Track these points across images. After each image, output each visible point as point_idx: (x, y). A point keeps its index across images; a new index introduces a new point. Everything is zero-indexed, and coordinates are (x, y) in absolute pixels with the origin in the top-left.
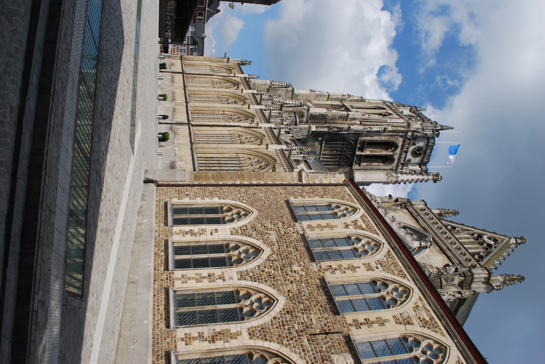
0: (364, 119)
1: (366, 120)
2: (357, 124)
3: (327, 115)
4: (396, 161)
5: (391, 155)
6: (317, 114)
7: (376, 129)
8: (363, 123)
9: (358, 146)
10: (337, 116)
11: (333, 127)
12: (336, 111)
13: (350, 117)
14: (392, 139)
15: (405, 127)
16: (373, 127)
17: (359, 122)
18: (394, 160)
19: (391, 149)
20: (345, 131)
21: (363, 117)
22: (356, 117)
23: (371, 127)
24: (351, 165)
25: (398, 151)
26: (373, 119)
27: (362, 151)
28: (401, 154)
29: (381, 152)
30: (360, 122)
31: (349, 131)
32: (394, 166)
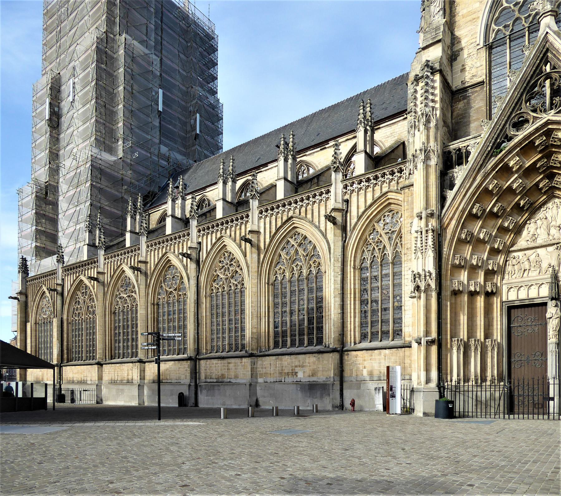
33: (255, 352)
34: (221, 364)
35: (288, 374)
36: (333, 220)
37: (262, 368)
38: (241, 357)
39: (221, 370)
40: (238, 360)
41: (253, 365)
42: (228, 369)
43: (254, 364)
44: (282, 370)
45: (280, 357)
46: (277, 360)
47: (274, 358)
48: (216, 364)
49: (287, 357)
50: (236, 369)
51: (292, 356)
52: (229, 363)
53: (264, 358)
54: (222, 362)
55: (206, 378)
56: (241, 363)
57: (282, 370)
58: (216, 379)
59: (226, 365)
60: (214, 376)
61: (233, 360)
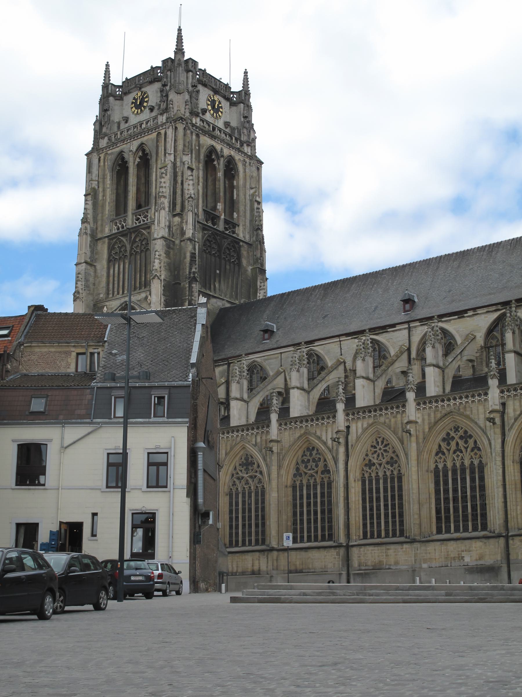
0: (169, 207)
1: (173, 204)
2: (182, 222)
3: (164, 280)
4: (233, 153)
5: (224, 161)
6: (163, 300)
7: (191, 187)
8: (178, 209)
9: (210, 224)
10: (166, 260)
11: (190, 273)
12: (157, 261)
13: (166, 235)
14: (202, 157)
15: (185, 129)
16: (186, 192)
17: (177, 219)
18: (231, 156)
19: (213, 160)
20: (195, 249)
21: (167, 209)
22: (167, 224)
23: (187, 196)
24: (237, 241)
25: (218, 147)
26: (170, 190)
27: (219, 217)
28: (223, 141)
29: (215, 180)
30: (174, 216)
31: (195, 241)
32: (240, 157)
33: (418, 538)
34: (378, 550)
35: (454, 558)
36: (492, 420)
37: (426, 553)
38: (402, 543)
39: (378, 556)
40: (398, 547)
41: (416, 550)
42: (386, 556)
43: (418, 550)
44: (448, 555)
45: (445, 542)
46: (443, 545)
47: (439, 543)
48: (372, 550)
49: (452, 542)
50: (396, 555)
51: (458, 542)
52: (388, 549)
53: (427, 544)
54: (379, 548)
55: (359, 566)
56: (402, 548)
57: (448, 555)
58: (372, 566)
59: (384, 551)
60: (369, 563)
61: (392, 547)
